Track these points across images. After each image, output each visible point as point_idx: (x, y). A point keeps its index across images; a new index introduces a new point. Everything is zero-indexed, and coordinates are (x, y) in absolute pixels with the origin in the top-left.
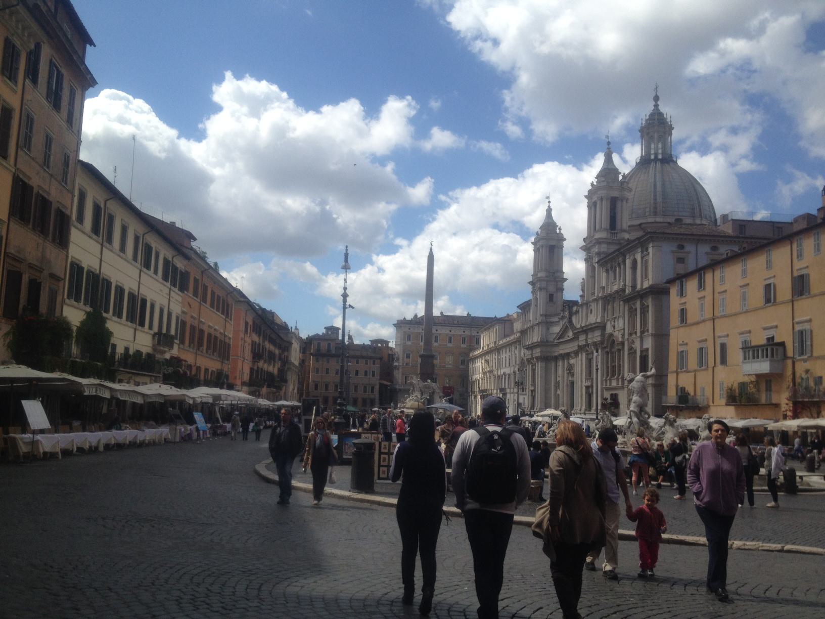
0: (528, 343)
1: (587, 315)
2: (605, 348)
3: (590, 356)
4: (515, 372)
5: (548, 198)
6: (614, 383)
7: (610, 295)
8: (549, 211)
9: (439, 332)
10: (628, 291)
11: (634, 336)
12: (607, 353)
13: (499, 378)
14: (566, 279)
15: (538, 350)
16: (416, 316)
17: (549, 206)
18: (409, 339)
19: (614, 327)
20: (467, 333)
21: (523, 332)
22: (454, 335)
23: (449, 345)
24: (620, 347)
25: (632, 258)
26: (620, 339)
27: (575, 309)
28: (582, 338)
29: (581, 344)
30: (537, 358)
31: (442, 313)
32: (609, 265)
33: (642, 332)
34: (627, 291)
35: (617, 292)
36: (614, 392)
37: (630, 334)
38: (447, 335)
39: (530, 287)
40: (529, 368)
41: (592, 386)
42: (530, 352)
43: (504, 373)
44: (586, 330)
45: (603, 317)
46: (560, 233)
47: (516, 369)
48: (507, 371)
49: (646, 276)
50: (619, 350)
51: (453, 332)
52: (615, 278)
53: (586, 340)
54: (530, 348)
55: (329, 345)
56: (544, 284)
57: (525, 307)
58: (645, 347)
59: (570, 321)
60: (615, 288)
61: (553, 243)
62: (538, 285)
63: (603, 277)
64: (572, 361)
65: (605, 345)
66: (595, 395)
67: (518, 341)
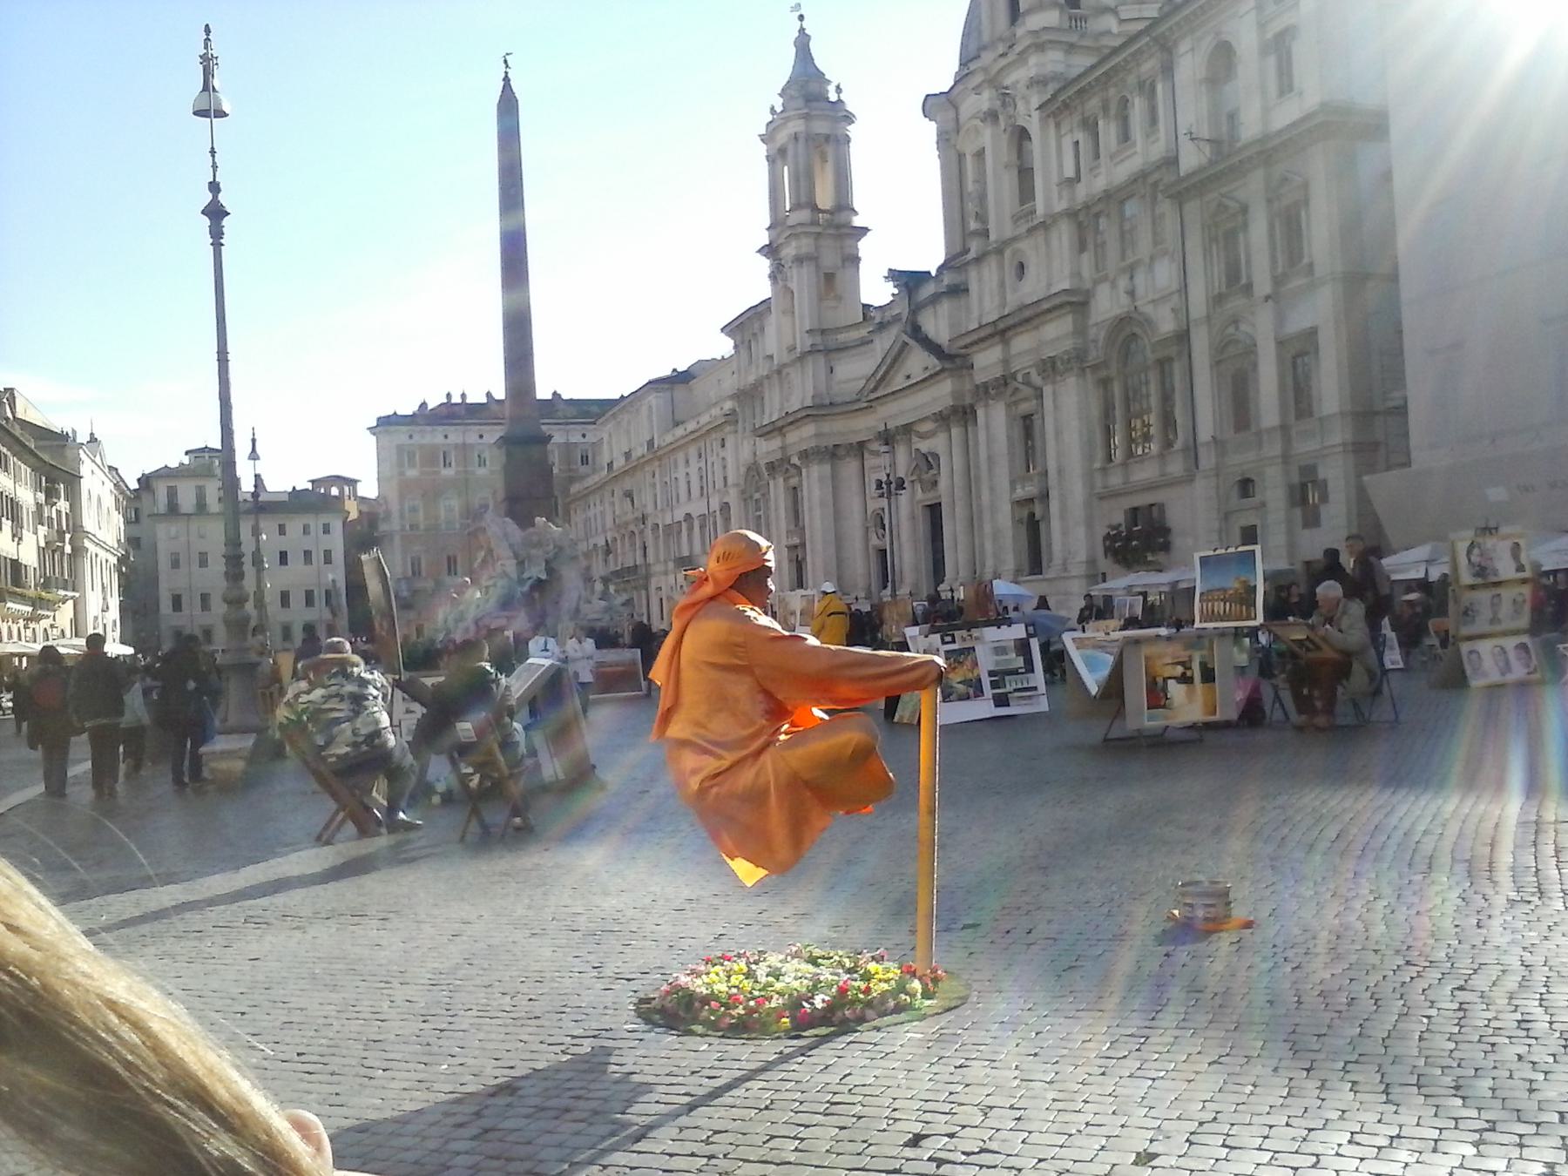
0: (772, 411)
1: (1002, 284)
2: (1095, 368)
3: (1025, 407)
4: (725, 507)
5: (799, 6)
6: (1144, 473)
7: (1107, 196)
8: (803, 43)
10: (1190, 159)
11: (1236, 303)
12: (1105, 383)
13: (672, 530)
14: (864, 231)
15: (809, 430)
16: (424, 405)
17: (802, 30)
18: (412, 464)
19: (1131, 293)
21: (749, 395)
24: (1172, 351)
25: (1207, 44)
26: (1166, 324)
27: (928, 290)
28: (987, 361)
29: (980, 378)
30: (804, 455)
32: (1094, 104)
33: (1278, 281)
34: (1190, 159)
35: (1141, 176)
36: (1141, 500)
37: (1218, 300)
39: (765, 264)
40: (778, 490)
41: (1045, 496)
42: (775, 443)
43: (688, 516)
44: (1001, 331)
45: (1077, 274)
46: (840, 101)
47: (733, 497)
48: (697, 508)
49: (1286, 86)
50: (1163, 364)
52: (1125, 136)
53: (1006, 362)
54: (775, 430)
56: (805, 245)
57: (745, 327)
58: (1298, 321)
59: (916, 331)
60: (1122, 172)
61: (821, 127)
62: (789, 252)
63: (1054, 154)
64: (924, 446)
65: (1094, 355)
66: (1055, 524)
67: (731, 418)
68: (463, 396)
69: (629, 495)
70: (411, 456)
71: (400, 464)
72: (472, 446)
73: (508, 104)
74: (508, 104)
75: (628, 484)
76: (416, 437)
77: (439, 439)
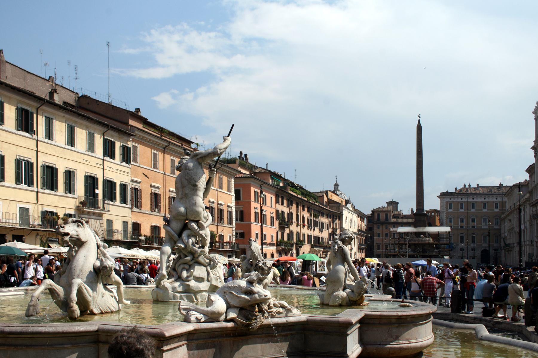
9: (475, 200)
18: (450, 208)
20: (499, 199)
22: (488, 202)
23: (484, 210)
31: (478, 185)
38: (482, 202)
51: (487, 199)
55: (386, 215)
68: (470, 185)
69: (510, 220)
70: (450, 205)
71: (447, 208)
72: (470, 202)
73: (419, 128)
74: (419, 128)
75: (510, 217)
76: (452, 199)
77: (459, 200)
